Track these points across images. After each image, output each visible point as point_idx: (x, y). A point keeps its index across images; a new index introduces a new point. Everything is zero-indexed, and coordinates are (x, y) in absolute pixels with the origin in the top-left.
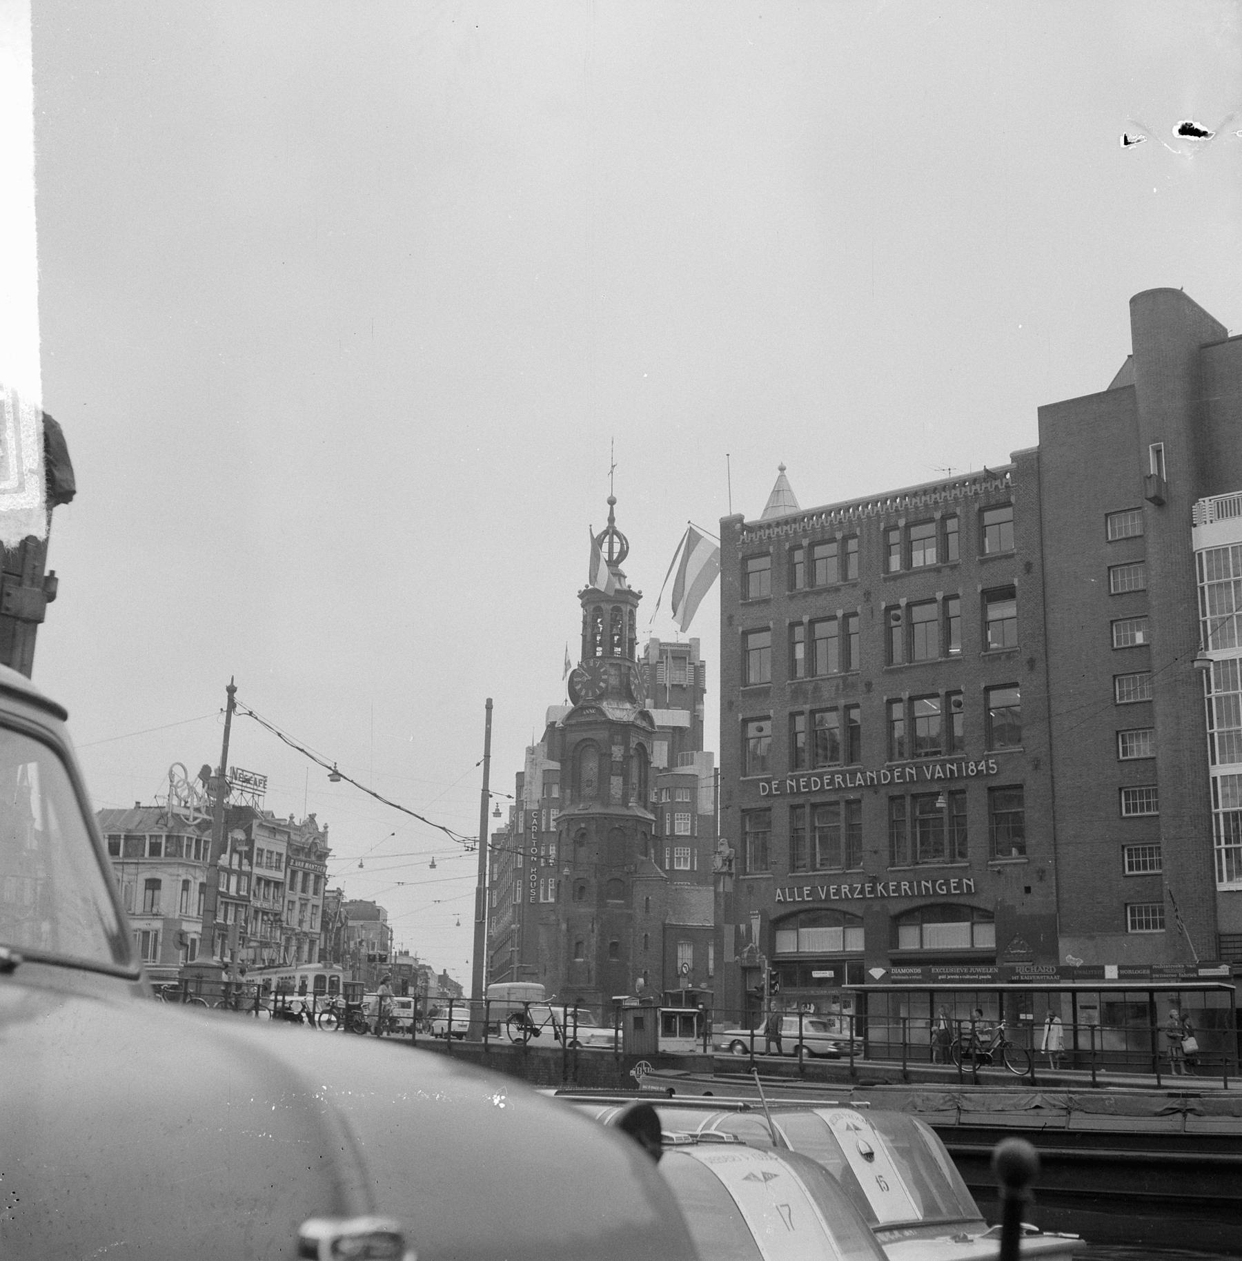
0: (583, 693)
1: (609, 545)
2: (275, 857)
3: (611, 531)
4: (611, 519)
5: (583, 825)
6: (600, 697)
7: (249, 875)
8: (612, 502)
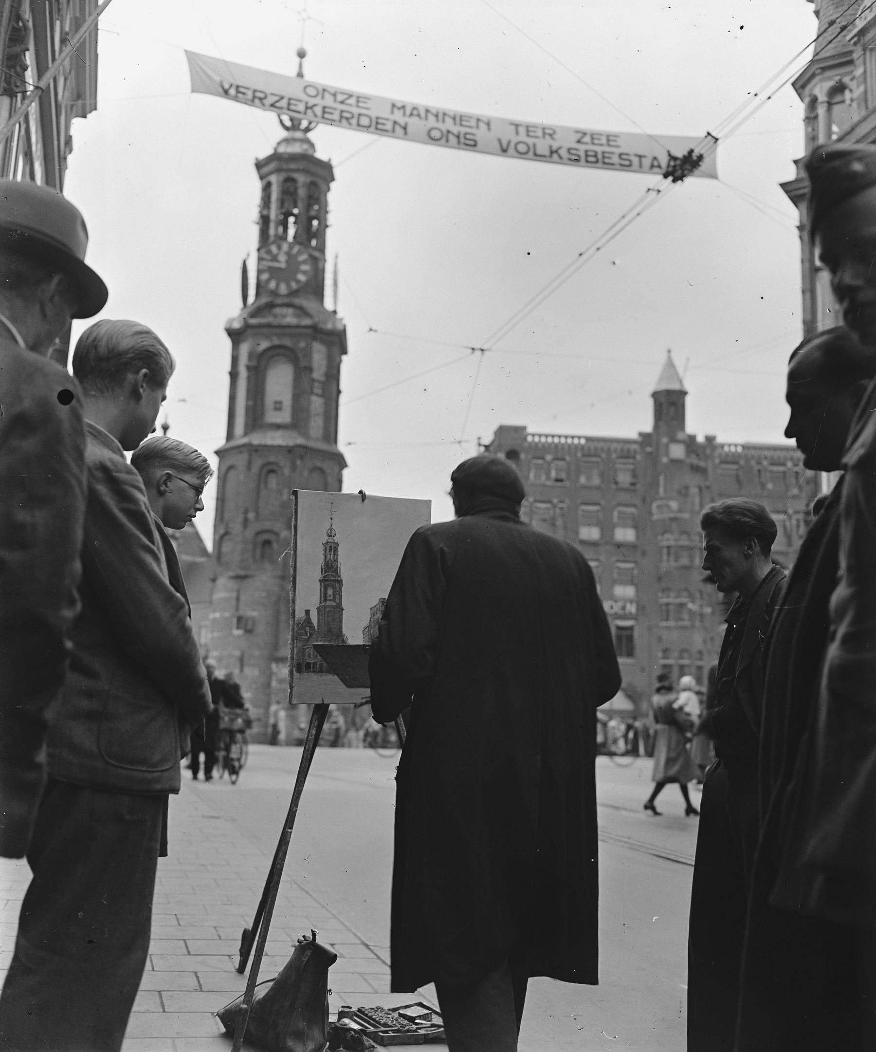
5: (272, 459)
8: (302, 55)
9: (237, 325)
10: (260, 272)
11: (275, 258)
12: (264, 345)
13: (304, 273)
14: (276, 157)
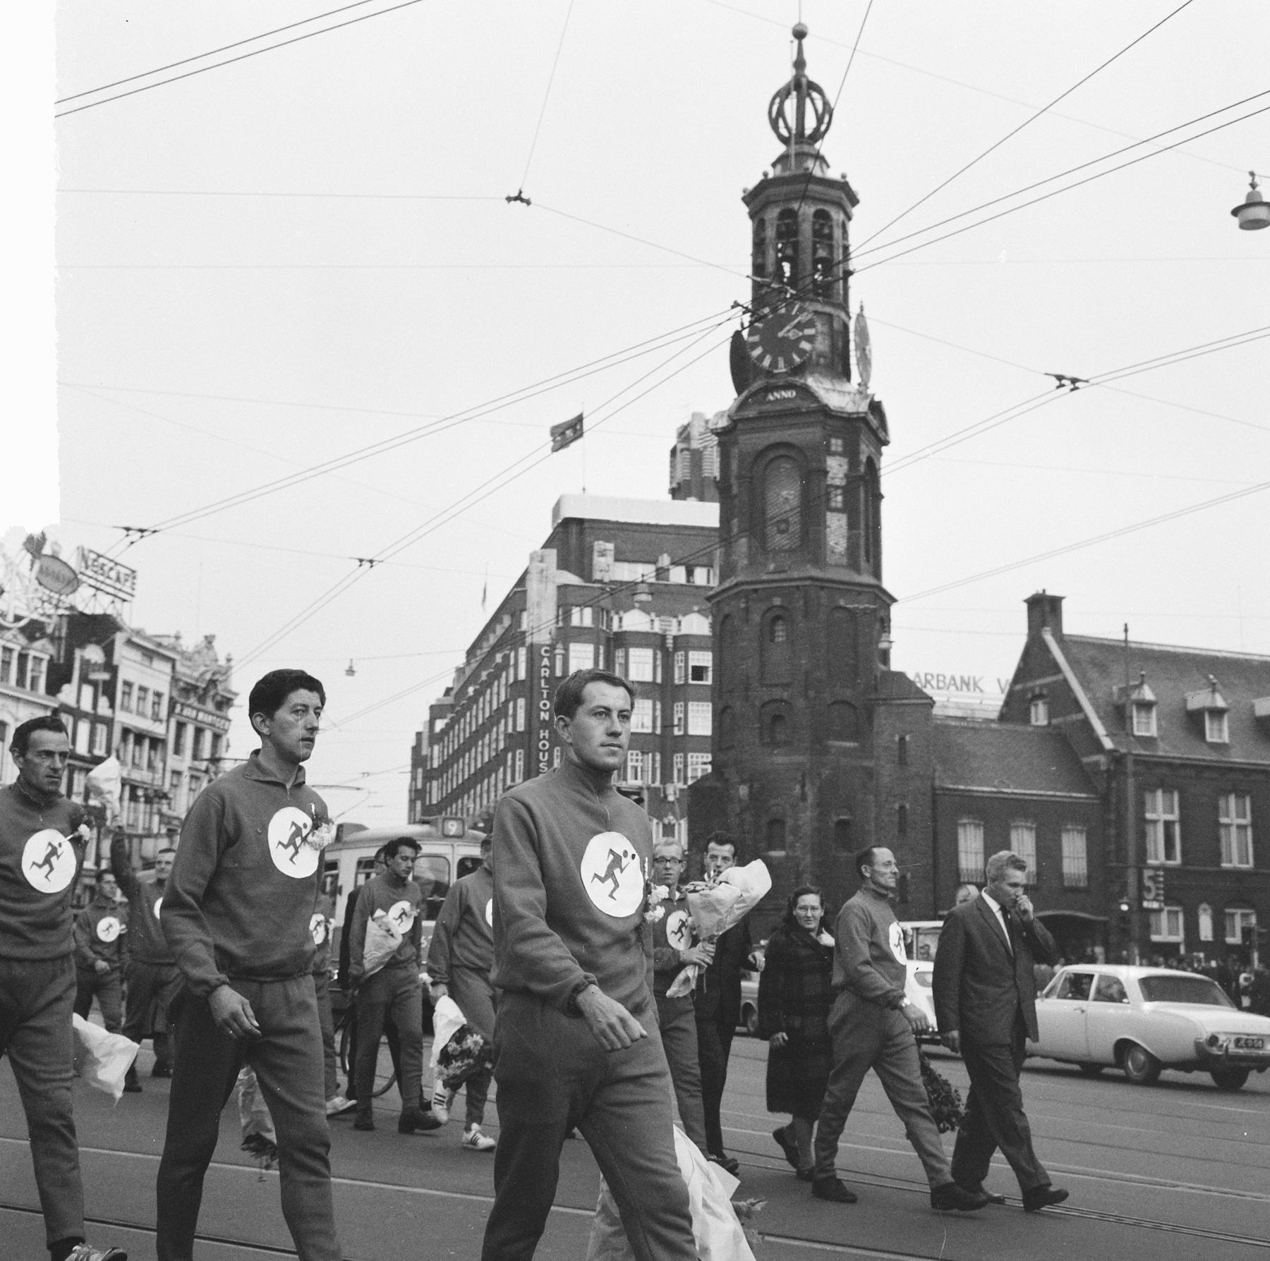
0: (767, 362)
2: (150, 698)
3: (801, 87)
4: (800, 64)
5: (777, 601)
6: (799, 370)
7: (109, 722)
8: (800, 34)
14: (765, 184)
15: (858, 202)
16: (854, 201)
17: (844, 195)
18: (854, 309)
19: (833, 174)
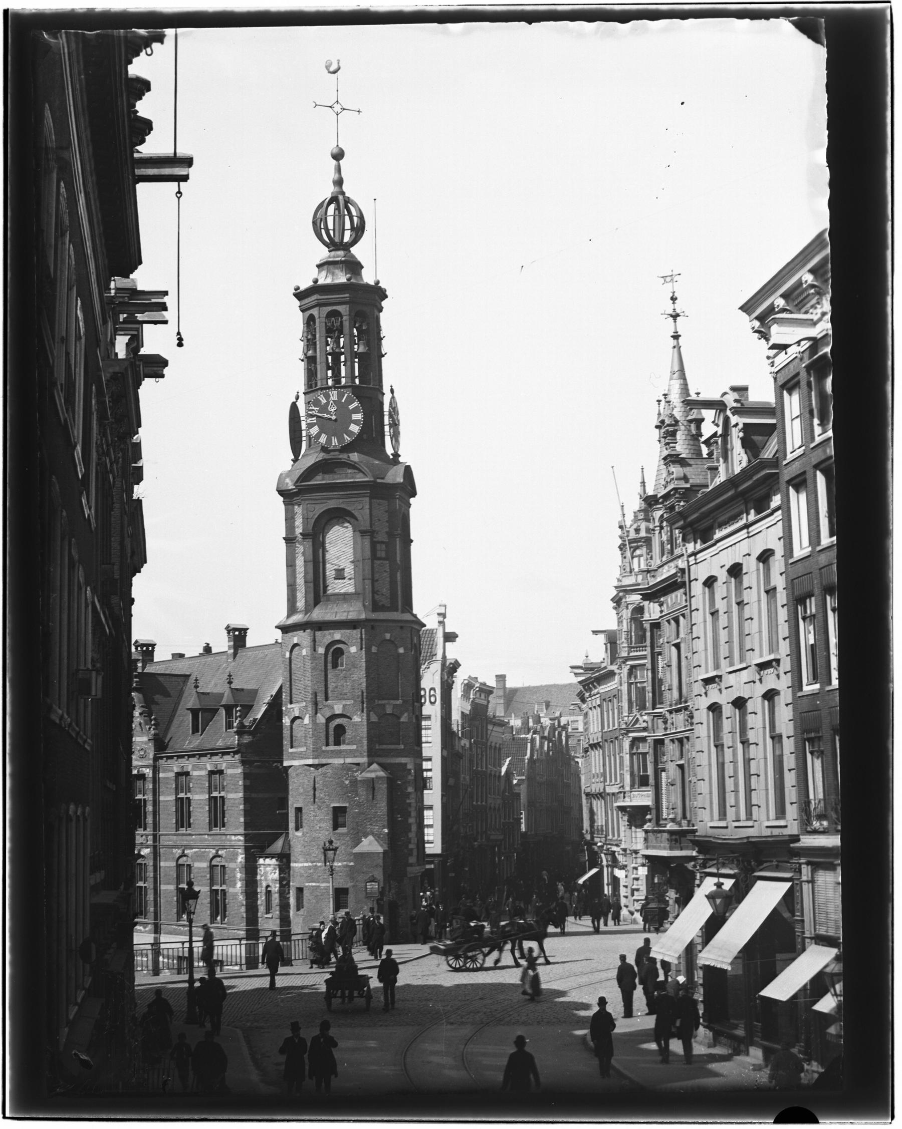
1: (340, 223)
4: (339, 182)
5: (337, 635)
8: (338, 156)
9: (290, 485)
10: (310, 426)
11: (324, 409)
12: (320, 509)
13: (356, 422)
14: (316, 289)
15: (387, 297)
16: (383, 295)
17: (378, 294)
18: (386, 389)
19: (368, 277)
